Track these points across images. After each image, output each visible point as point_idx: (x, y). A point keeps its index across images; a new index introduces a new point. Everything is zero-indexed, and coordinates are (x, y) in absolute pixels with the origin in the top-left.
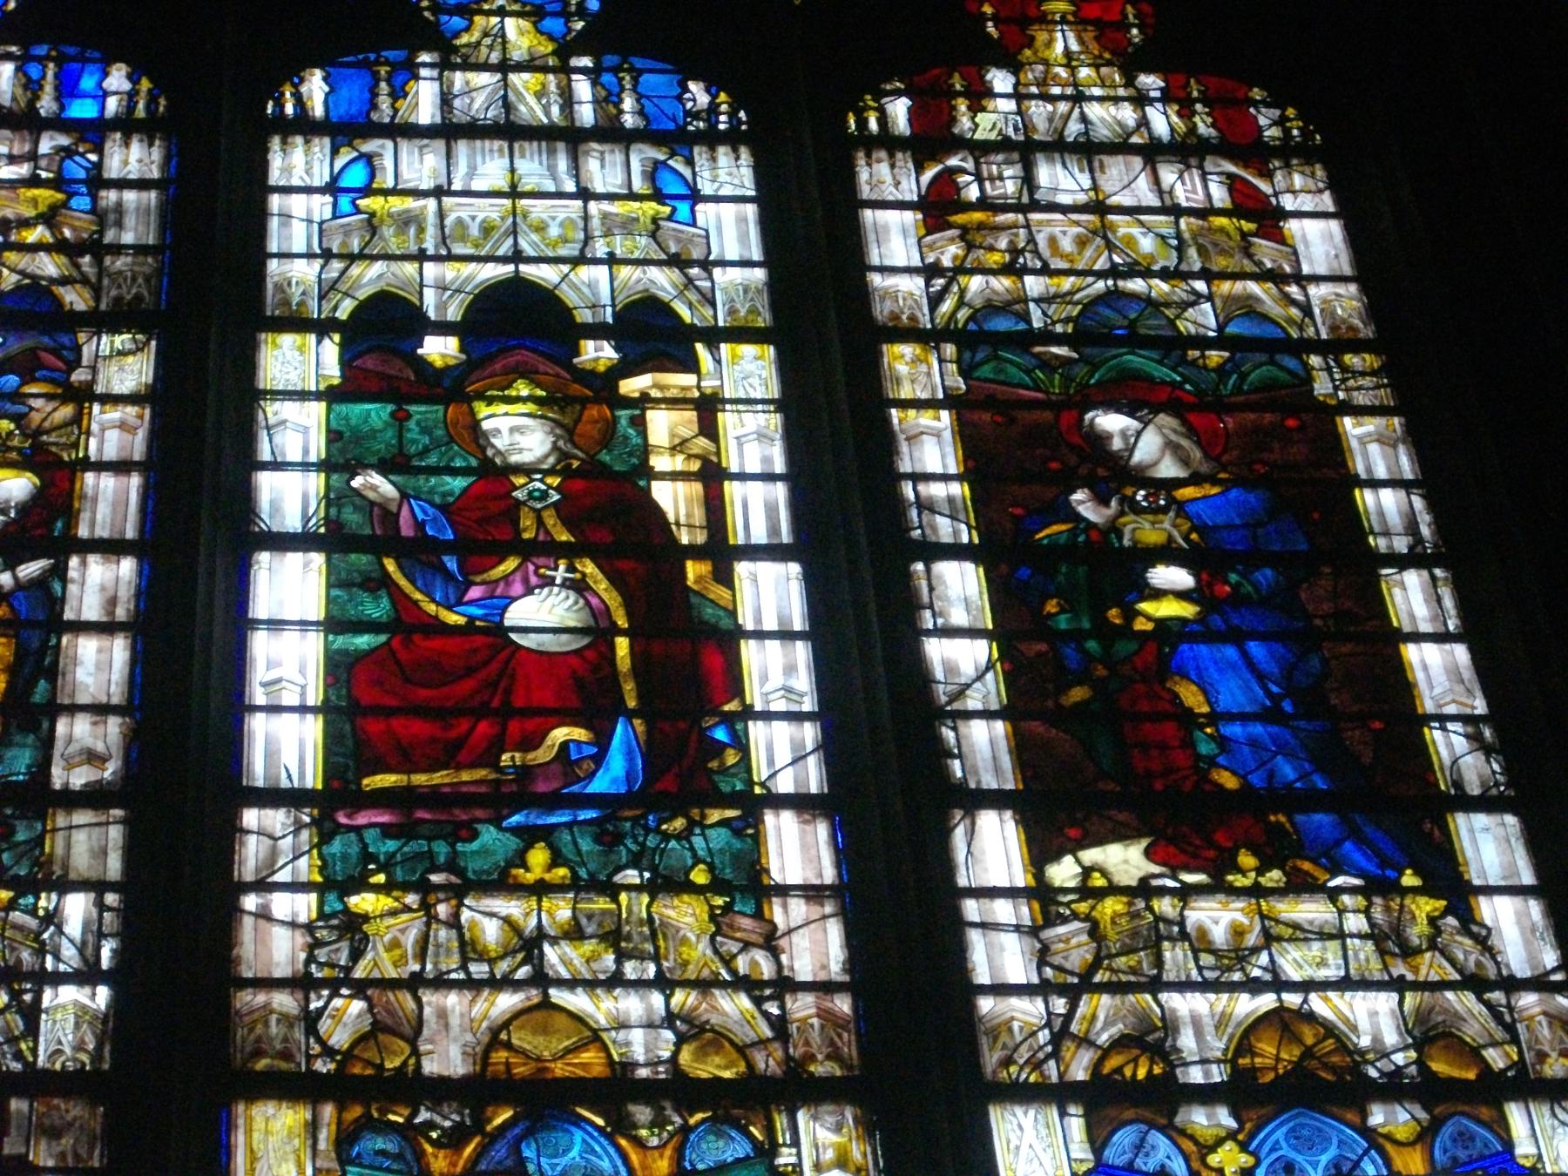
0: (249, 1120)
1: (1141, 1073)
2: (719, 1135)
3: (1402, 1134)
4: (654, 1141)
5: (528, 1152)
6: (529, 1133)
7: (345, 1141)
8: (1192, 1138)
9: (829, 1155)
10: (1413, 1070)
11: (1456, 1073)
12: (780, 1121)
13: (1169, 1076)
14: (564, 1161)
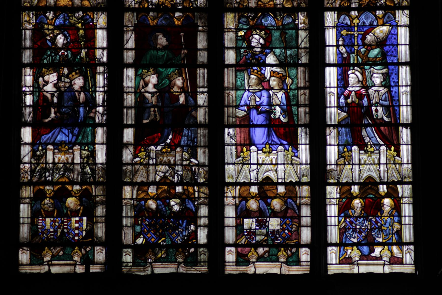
0: (227, 15)
1: (346, 5)
2: (288, 18)
3: (380, 16)
4: (279, 19)
5: (263, 21)
6: (263, 18)
7: (239, 19)
8: (351, 17)
9: (302, 21)
10: (384, 4)
11: (390, 4)
12: (296, 15)
13: (350, 5)
14: (267, 23)
